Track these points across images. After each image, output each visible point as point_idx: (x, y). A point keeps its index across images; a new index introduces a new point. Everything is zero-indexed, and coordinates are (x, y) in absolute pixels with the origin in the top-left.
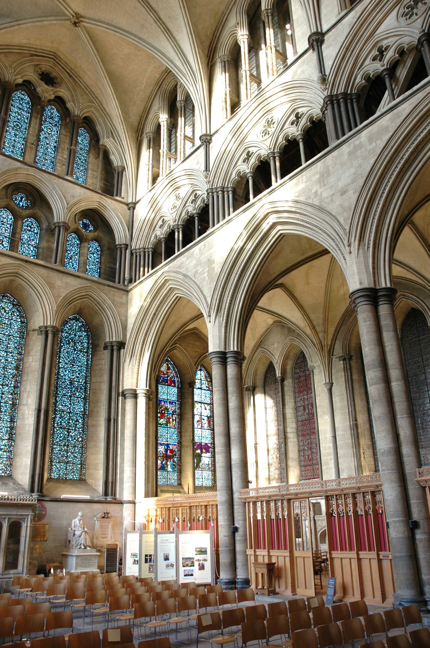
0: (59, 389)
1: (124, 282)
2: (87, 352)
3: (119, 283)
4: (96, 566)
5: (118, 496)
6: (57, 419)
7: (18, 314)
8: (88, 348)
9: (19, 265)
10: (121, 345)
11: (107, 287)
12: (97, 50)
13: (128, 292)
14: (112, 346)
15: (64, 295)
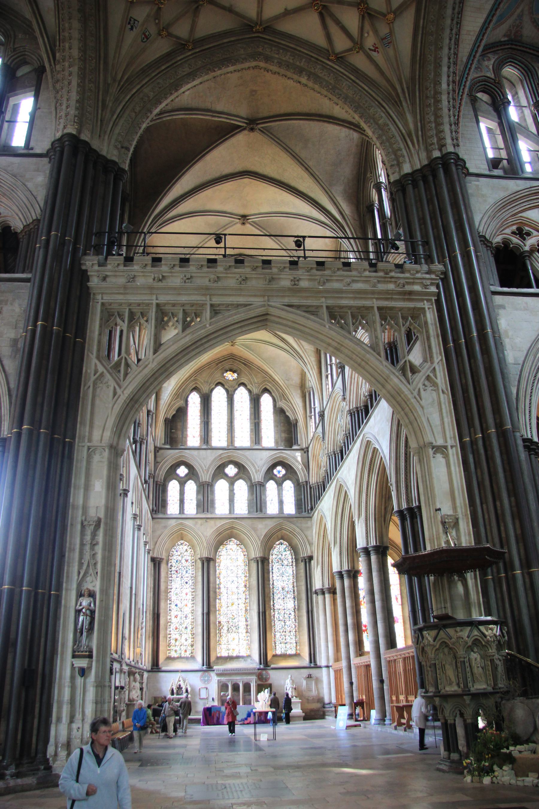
0: (275, 595)
1: (308, 511)
2: (292, 565)
3: (305, 512)
4: (300, 708)
5: (318, 664)
6: (276, 615)
7: (241, 550)
8: (292, 562)
9: (233, 522)
10: (311, 558)
11: (295, 519)
12: (253, 351)
13: (311, 517)
14: (305, 560)
15: (264, 534)
